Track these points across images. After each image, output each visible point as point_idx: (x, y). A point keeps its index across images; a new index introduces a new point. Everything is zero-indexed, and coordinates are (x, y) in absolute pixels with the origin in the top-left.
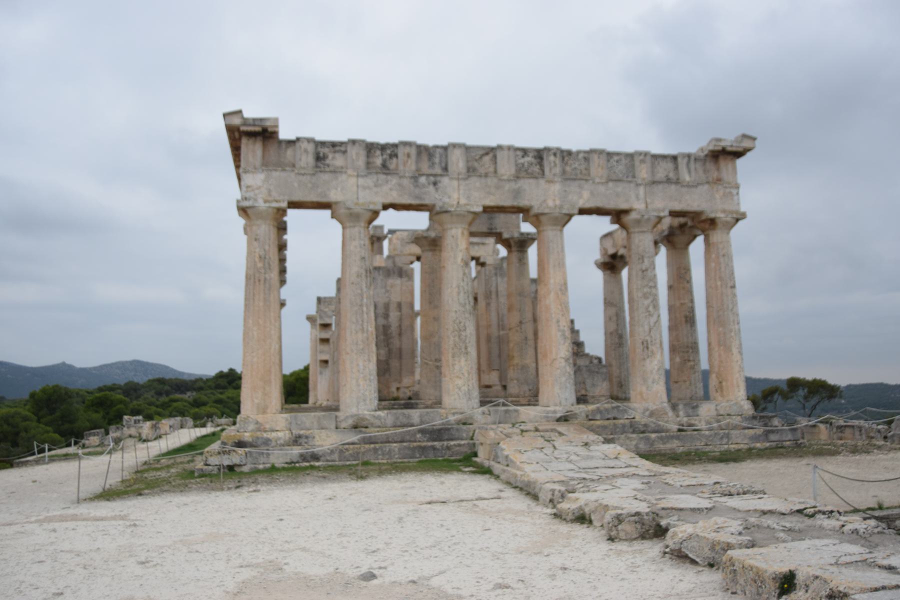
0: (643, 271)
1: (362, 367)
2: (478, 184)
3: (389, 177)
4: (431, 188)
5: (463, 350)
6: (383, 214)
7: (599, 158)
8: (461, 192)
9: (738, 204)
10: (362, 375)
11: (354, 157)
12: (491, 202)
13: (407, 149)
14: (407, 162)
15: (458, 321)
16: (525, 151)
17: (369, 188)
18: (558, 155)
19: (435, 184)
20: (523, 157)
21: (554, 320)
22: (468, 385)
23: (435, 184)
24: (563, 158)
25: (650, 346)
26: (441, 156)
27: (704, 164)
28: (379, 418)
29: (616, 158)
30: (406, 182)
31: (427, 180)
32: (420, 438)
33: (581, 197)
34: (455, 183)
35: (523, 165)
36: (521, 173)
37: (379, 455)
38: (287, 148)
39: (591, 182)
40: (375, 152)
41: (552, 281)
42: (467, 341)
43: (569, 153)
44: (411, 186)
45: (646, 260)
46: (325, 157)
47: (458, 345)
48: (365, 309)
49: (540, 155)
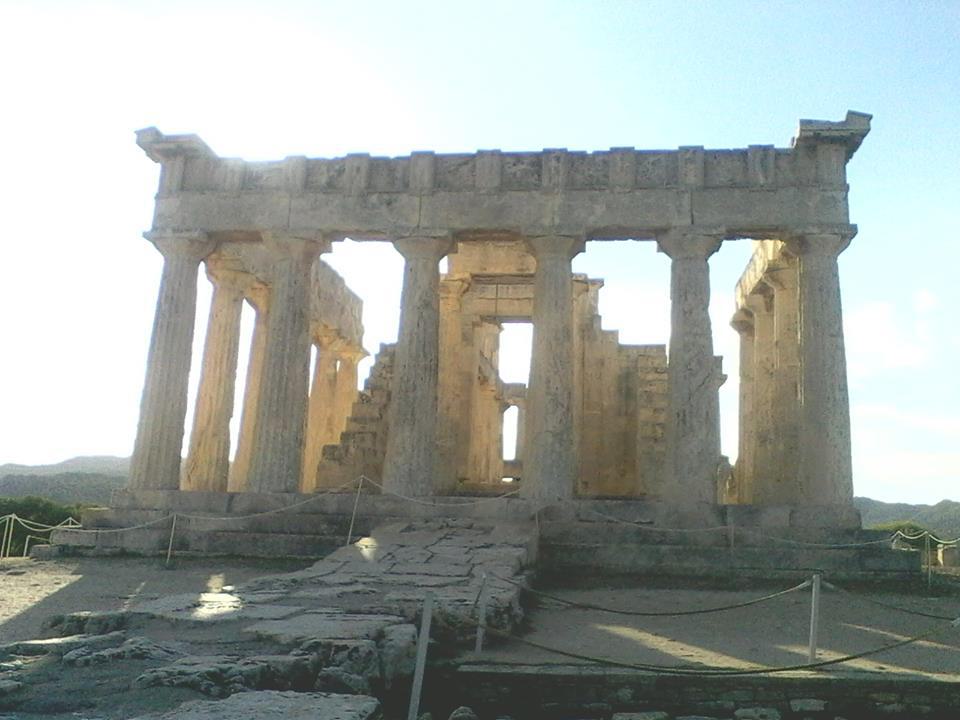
4: (384, 209)
5: (409, 417)
7: (622, 159)
9: (847, 214)
12: (458, 225)
15: (406, 379)
16: (518, 157)
18: (562, 160)
19: (389, 204)
20: (514, 165)
23: (389, 204)
25: (688, 418)
34: (416, 200)
35: (515, 174)
36: (507, 184)
39: (607, 191)
43: (582, 155)
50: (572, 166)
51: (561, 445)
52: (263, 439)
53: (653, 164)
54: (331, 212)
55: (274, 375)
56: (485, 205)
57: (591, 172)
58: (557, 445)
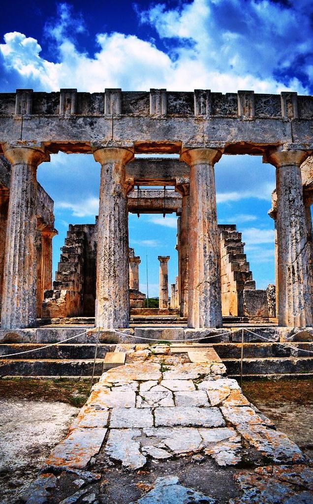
0: (290, 201)
1: (17, 288)
2: (131, 123)
3: (50, 120)
4: (88, 127)
6: (57, 158)
15: (108, 247)
16: (177, 95)
17: (32, 129)
19: (91, 124)
20: (175, 100)
22: (115, 307)
23: (91, 124)
24: (213, 100)
25: (296, 272)
28: (28, 334)
29: (264, 100)
30: (65, 123)
31: (83, 121)
32: (61, 355)
35: (175, 107)
37: (16, 371)
40: (42, 101)
41: (200, 210)
42: (116, 266)
43: (219, 95)
44: (70, 127)
47: (106, 269)
49: (189, 98)
50: (214, 102)
51: (216, 291)
52: (10, 290)
53: (265, 103)
56: (157, 127)
57: (226, 107)
58: (213, 291)
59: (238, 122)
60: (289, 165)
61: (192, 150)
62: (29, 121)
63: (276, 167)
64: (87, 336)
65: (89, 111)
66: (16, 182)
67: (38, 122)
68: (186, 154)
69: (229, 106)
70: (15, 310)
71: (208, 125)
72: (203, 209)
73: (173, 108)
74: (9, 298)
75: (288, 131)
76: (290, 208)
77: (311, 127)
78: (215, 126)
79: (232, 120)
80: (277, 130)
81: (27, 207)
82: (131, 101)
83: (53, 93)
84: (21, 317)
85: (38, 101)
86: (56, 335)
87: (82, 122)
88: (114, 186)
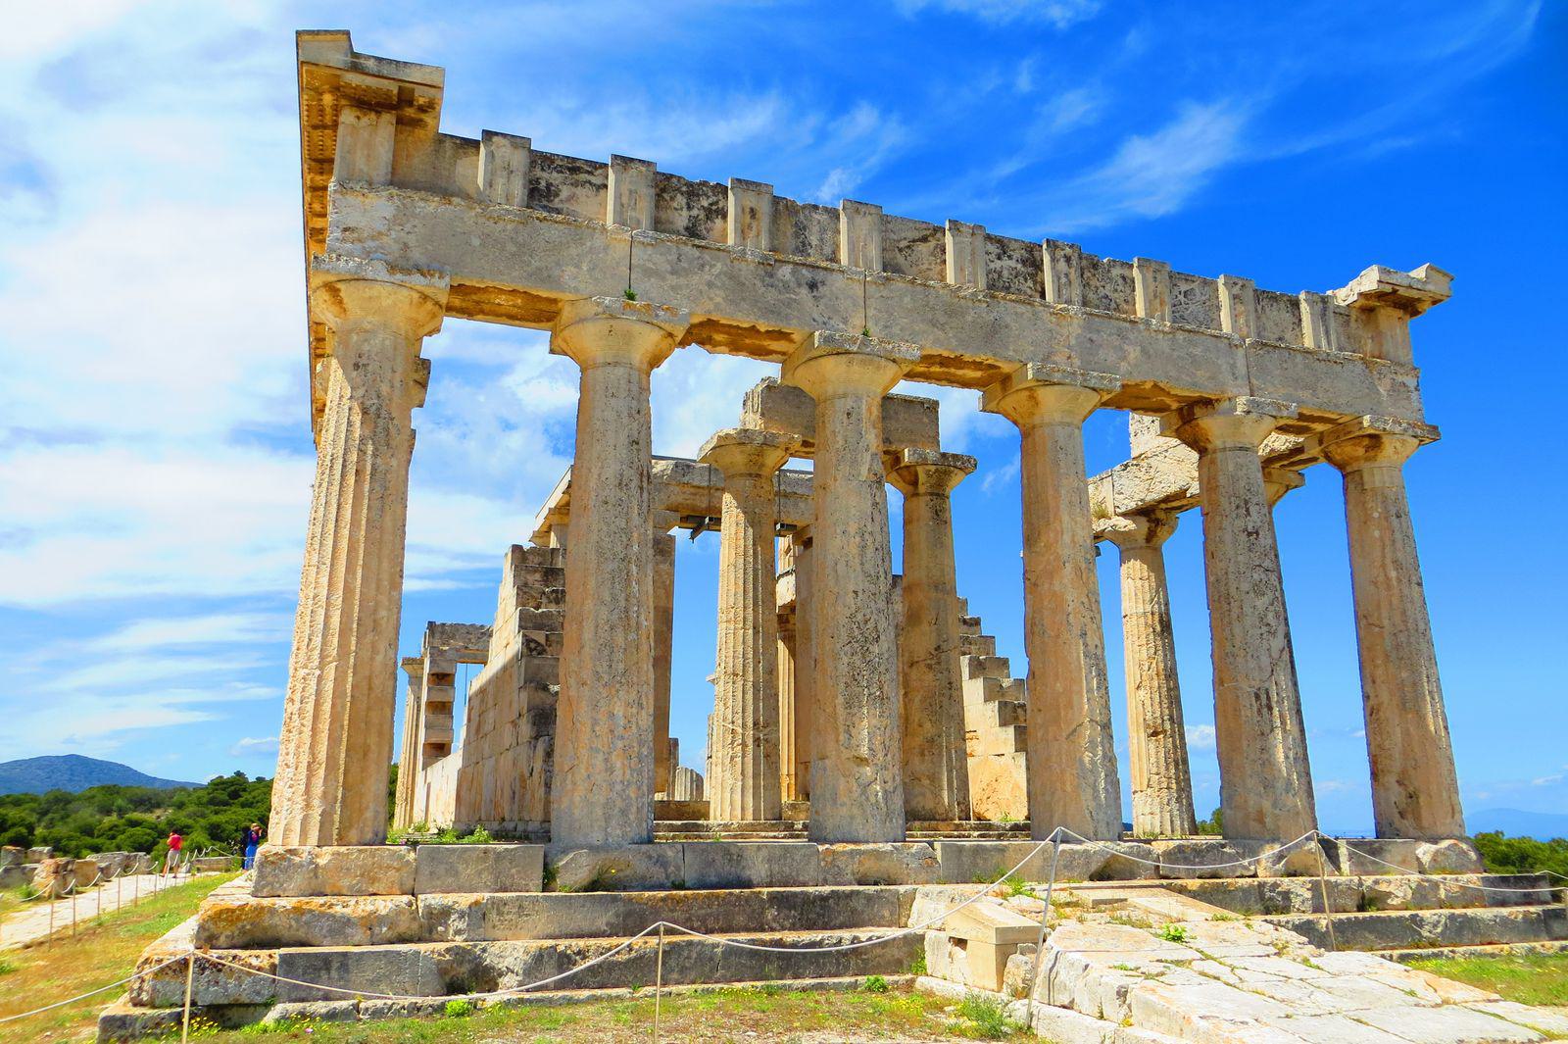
0: (1250, 534)
2: (907, 300)
4: (804, 291)
8: (871, 312)
10: (620, 744)
11: (625, 200)
13: (750, 200)
14: (750, 227)
15: (860, 617)
20: (999, 258)
21: (1076, 631)
26: (823, 231)
27: (1347, 323)
31: (793, 273)
32: (774, 920)
33: (1124, 358)
38: (455, 157)
40: (672, 199)
41: (1067, 538)
42: (882, 669)
44: (759, 283)
45: (1253, 509)
46: (550, 192)
48: (634, 569)
52: (602, 729)
54: (710, 285)
55: (614, 598)
56: (969, 318)
59: (1140, 332)
60: (1241, 449)
61: (1048, 388)
62: (650, 250)
63: (1202, 452)
64: (823, 864)
65: (797, 248)
66: (610, 415)
67: (675, 257)
68: (1027, 393)
69: (1116, 290)
70: (618, 787)
71: (1080, 332)
72: (1073, 536)
73: (996, 276)
74: (597, 751)
75: (1242, 370)
76: (1250, 550)
77: (1285, 366)
78: (1094, 337)
79: (1128, 325)
80: (1219, 362)
81: (641, 488)
82: (899, 241)
83: (704, 183)
84: (634, 810)
85: (663, 198)
86: (739, 862)
87: (788, 277)
88: (867, 457)
